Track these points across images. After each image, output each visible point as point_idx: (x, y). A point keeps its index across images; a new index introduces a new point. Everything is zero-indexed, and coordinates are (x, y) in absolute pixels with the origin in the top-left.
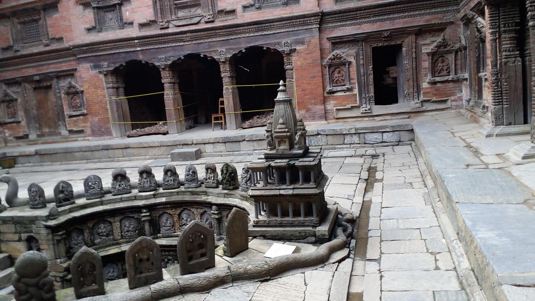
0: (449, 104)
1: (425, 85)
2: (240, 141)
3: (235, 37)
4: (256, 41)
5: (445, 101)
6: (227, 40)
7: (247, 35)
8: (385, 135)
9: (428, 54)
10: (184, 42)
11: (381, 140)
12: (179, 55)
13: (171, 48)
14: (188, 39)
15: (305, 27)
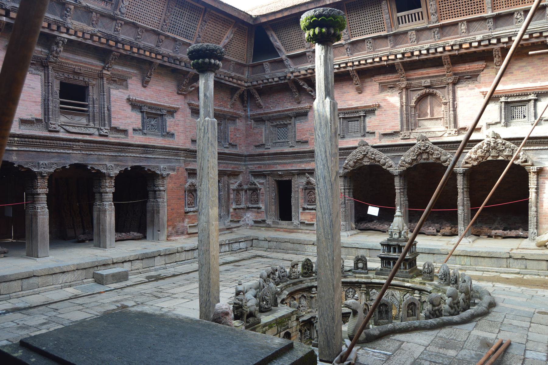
0: (241, 223)
1: (231, 210)
2: (154, 257)
3: (123, 154)
4: (140, 162)
5: (238, 221)
6: (116, 156)
7: (134, 155)
8: (241, 243)
9: (234, 190)
10: (73, 150)
11: (238, 248)
12: (64, 164)
13: (56, 154)
14: (79, 148)
15: (176, 158)
